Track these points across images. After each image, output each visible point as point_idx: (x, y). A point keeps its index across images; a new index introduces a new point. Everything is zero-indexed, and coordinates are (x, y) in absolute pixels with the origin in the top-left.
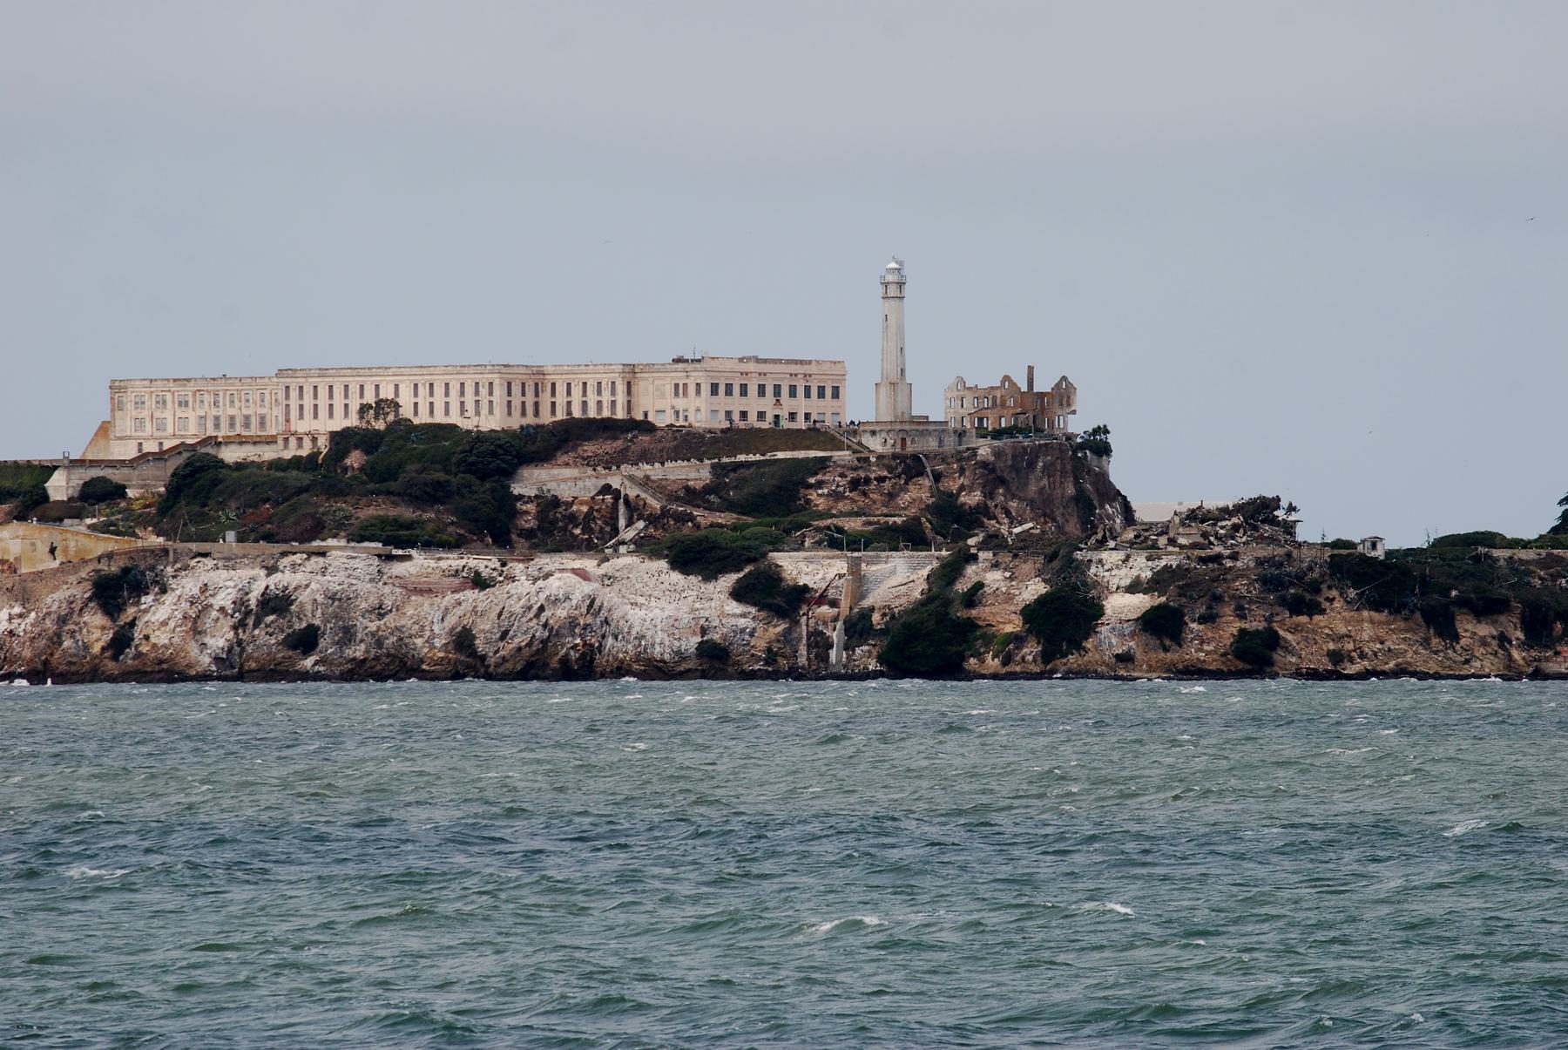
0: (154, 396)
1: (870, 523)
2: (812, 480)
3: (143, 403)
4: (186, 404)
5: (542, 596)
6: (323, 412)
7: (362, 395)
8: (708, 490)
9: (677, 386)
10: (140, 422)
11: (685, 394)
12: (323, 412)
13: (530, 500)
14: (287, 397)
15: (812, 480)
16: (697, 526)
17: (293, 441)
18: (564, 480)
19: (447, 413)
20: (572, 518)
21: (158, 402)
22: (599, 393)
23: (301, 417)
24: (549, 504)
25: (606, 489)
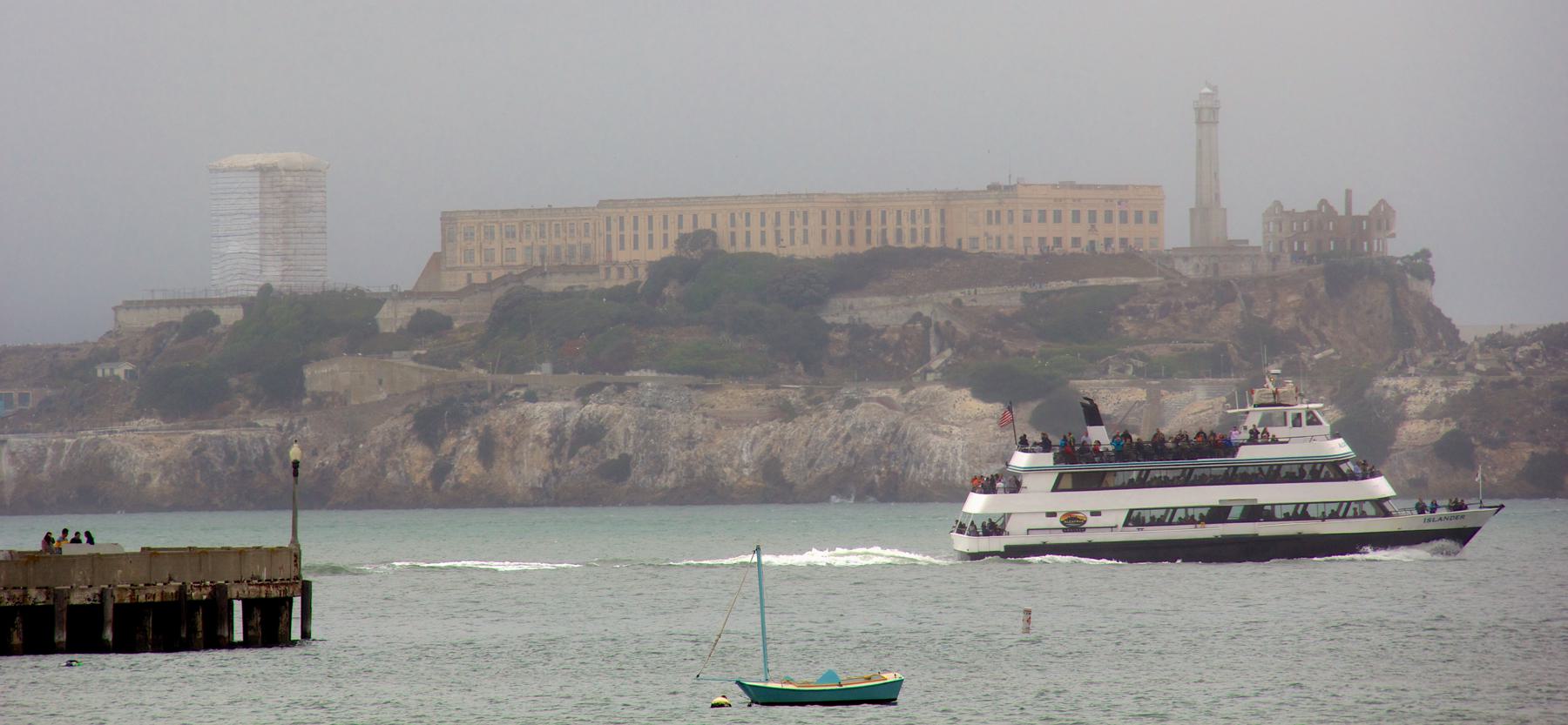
3: (472, 234)
4: (514, 235)
5: (848, 426)
7: (680, 226)
9: (990, 213)
11: (998, 221)
14: (609, 228)
15: (1122, 307)
17: (614, 272)
23: (622, 247)
24: (860, 332)
25: (918, 316)
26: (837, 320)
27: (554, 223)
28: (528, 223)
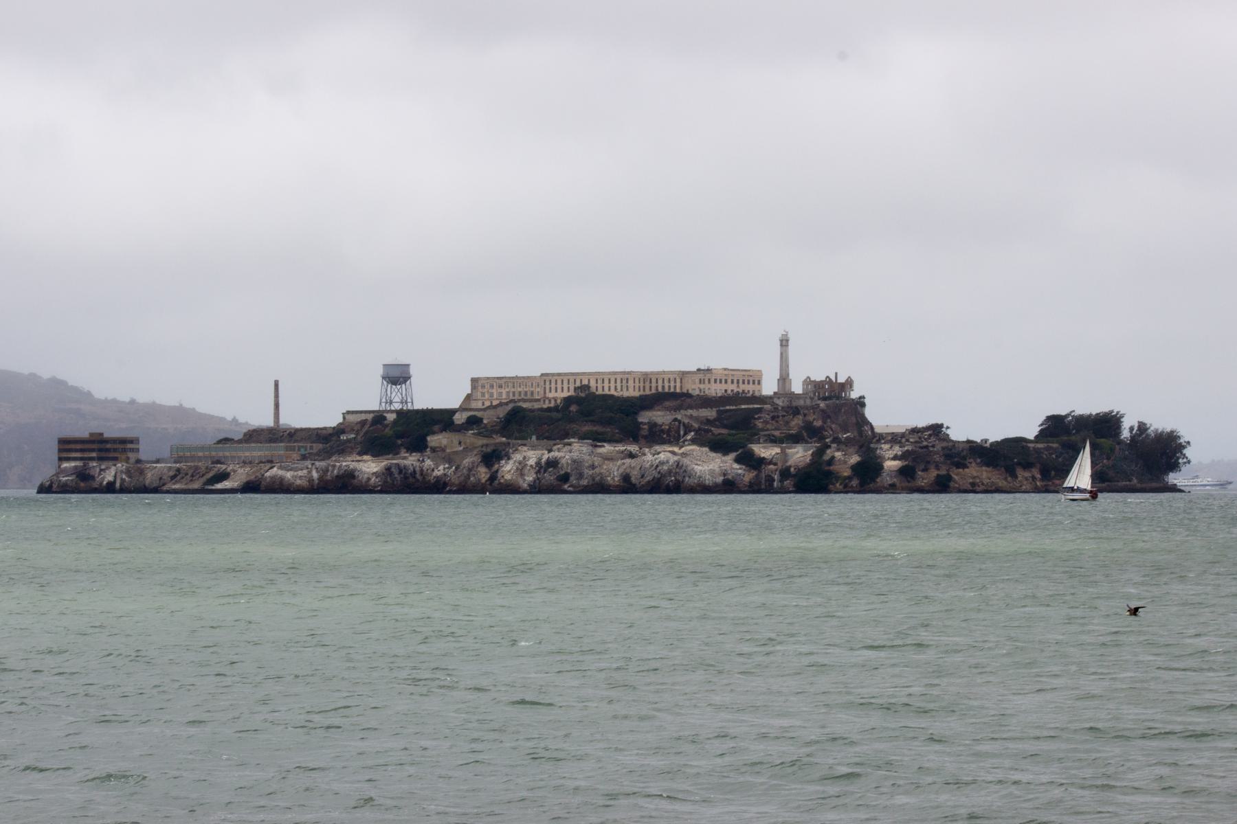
4: (502, 387)
5: (657, 461)
6: (559, 390)
7: (575, 384)
9: (700, 380)
10: (483, 394)
11: (704, 383)
12: (559, 390)
13: (645, 424)
14: (545, 384)
15: (756, 416)
16: (713, 434)
17: (547, 402)
18: (660, 416)
19: (609, 390)
20: (663, 431)
22: (669, 382)
23: (550, 391)
24: (653, 425)
25: (676, 420)
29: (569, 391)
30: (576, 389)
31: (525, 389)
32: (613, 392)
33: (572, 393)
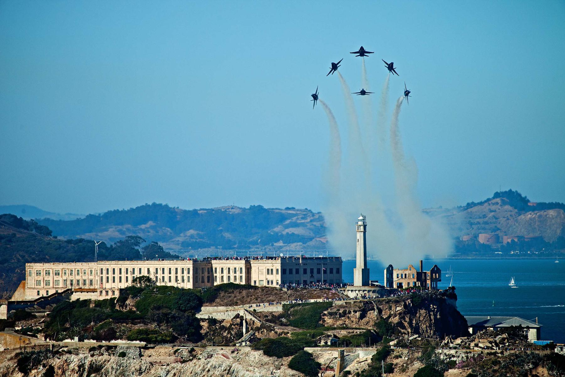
0: (45, 271)
1: (349, 333)
2: (326, 312)
3: (40, 273)
4: (59, 274)
5: (209, 366)
6: (117, 280)
7: (134, 273)
8: (281, 316)
9: (268, 270)
10: (38, 283)
11: (272, 273)
12: (117, 280)
14: (102, 273)
15: (326, 312)
16: (276, 333)
17: (104, 292)
18: (220, 312)
19: (170, 281)
20: (223, 328)
21: (46, 273)
22: (235, 272)
23: (108, 281)
24: (212, 322)
25: (237, 316)
26: (202, 317)
27: (76, 269)
28: (65, 269)
29: (127, 281)
30: (134, 280)
31: (83, 278)
32: (173, 284)
33: (130, 284)
